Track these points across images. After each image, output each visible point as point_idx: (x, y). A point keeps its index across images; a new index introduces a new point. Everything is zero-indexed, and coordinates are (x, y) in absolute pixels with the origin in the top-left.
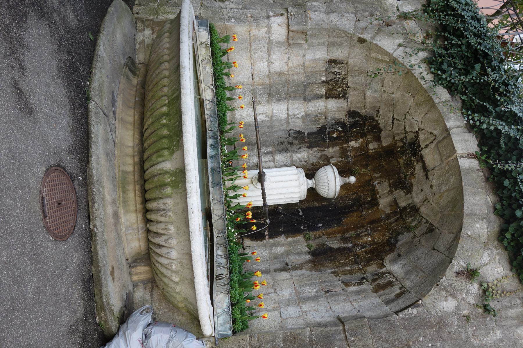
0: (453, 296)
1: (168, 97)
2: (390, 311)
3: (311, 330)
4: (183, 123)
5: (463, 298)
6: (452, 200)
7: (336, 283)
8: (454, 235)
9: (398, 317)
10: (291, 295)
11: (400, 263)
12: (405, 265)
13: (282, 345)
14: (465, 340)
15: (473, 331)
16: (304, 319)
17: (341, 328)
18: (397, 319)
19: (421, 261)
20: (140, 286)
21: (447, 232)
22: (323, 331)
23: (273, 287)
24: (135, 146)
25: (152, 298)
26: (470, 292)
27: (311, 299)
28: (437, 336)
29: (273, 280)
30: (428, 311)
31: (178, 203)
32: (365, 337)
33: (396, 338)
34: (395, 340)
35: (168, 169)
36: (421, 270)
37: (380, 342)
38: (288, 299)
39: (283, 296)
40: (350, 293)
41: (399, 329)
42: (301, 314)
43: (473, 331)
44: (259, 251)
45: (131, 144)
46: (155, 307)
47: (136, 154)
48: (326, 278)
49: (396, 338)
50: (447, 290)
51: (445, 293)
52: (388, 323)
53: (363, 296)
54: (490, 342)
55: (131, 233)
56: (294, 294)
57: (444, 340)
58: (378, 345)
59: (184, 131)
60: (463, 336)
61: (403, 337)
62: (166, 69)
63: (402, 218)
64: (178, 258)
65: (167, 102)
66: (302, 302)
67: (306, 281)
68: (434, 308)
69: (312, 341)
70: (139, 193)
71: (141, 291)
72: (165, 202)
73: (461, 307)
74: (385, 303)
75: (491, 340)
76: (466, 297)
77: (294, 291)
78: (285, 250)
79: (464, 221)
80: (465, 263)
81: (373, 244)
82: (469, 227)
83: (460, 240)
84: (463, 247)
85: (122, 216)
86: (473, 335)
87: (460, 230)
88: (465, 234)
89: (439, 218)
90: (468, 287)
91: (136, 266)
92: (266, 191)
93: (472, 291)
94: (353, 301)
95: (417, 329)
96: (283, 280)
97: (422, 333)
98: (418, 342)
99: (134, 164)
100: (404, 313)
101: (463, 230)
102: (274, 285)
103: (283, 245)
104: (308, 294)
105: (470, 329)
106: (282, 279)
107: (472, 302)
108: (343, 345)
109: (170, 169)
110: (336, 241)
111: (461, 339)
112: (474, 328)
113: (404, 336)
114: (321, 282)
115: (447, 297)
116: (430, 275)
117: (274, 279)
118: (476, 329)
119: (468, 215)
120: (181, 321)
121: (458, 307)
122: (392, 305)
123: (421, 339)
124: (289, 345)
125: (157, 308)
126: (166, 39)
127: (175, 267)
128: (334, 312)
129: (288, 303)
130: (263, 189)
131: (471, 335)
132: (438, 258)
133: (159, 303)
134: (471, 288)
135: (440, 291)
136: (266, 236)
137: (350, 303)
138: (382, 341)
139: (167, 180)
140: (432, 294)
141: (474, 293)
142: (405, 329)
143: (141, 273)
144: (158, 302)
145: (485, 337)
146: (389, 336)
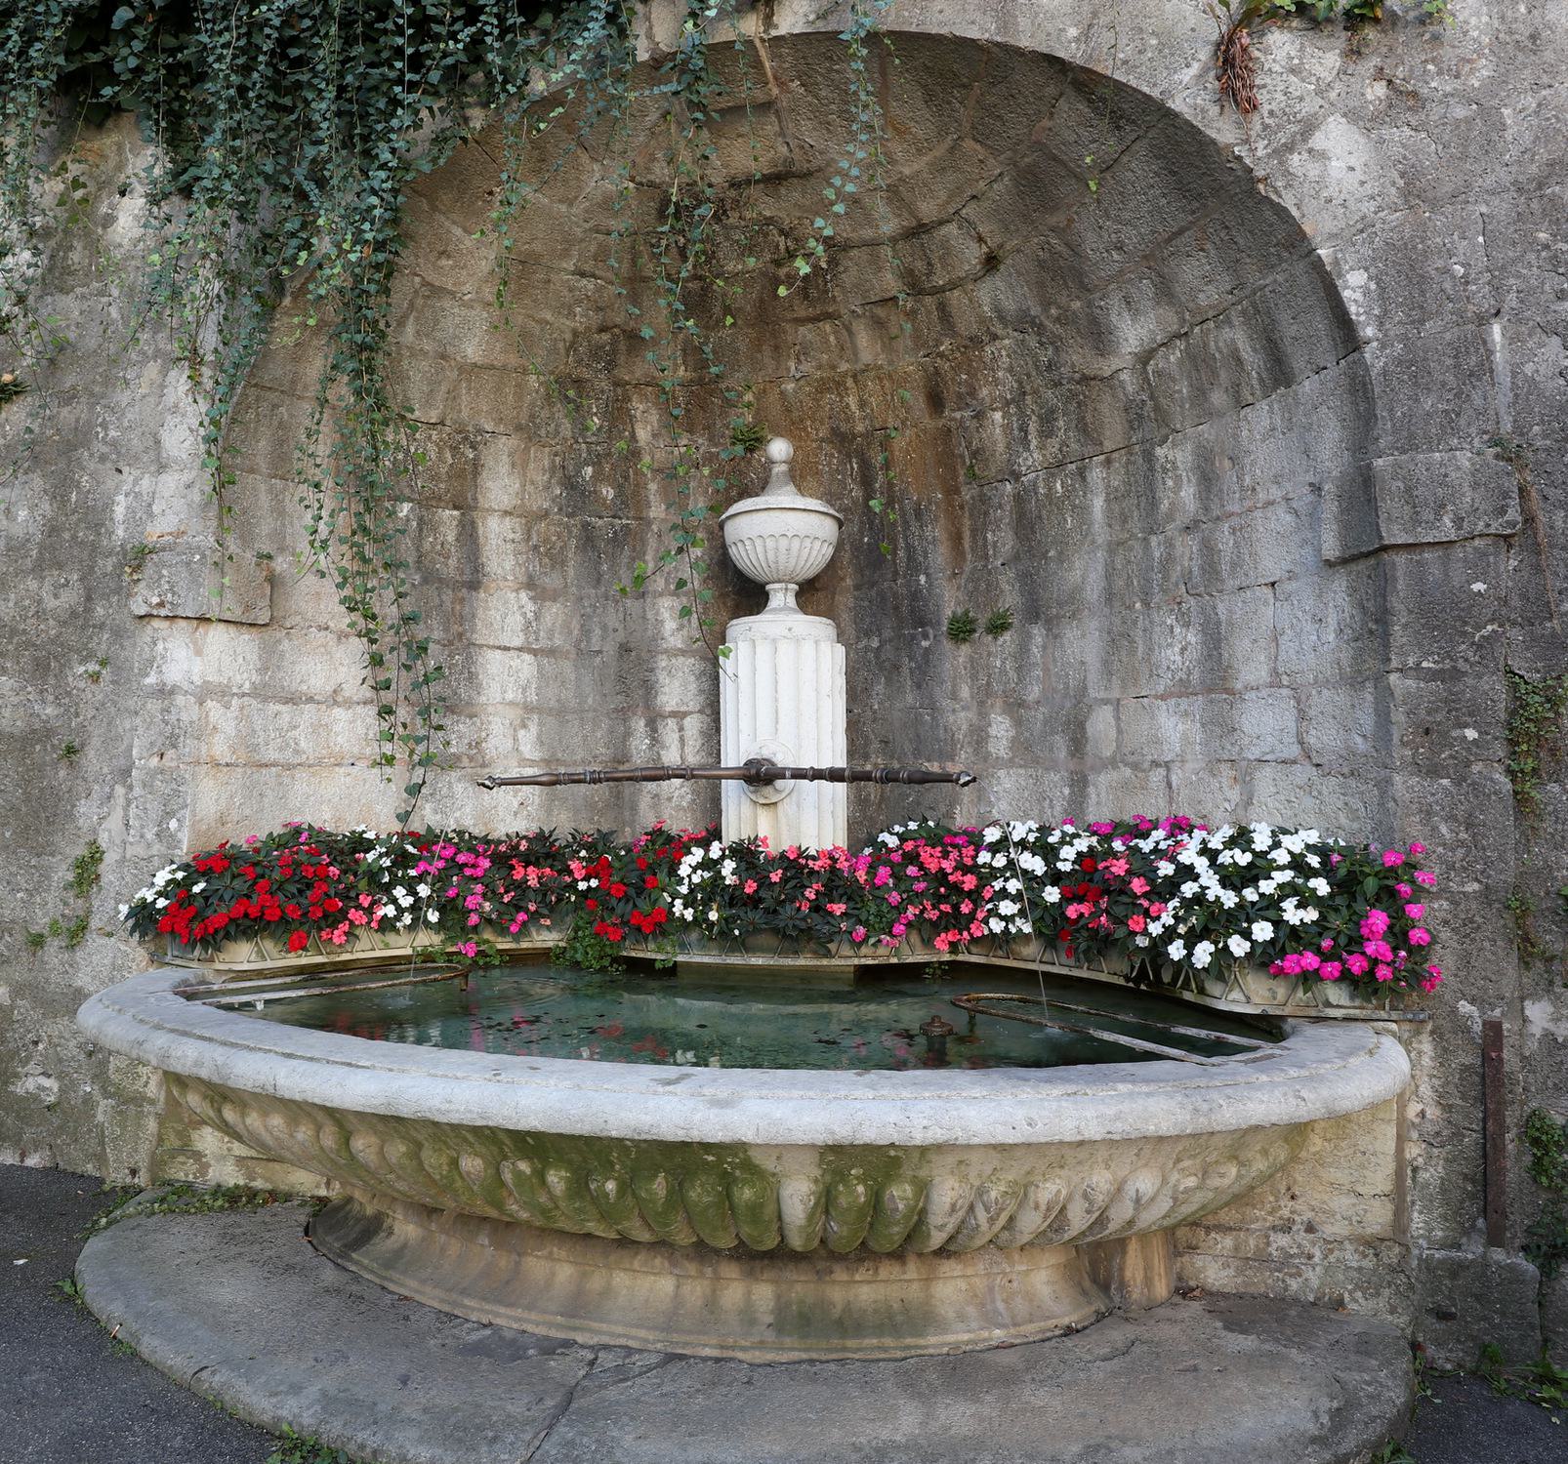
0: (1309, 127)
1: (505, 1158)
2: (1333, 372)
3: (1401, 671)
4: (644, 1137)
5: (1319, 92)
6: (924, 87)
7: (1157, 554)
8: (1070, 91)
9: (1375, 344)
10: (1186, 714)
11: (1114, 318)
12: (1128, 301)
13: (1445, 782)
14: (1475, 106)
15: (1440, 73)
16: (1320, 683)
17: (1400, 559)
18: (1383, 347)
19: (1131, 237)
20: (1182, 1269)
21: (1046, 123)
22: (1405, 626)
23: (1144, 771)
24: (676, 1271)
25: (1231, 1229)
26: (1296, 61)
27: (1217, 648)
28: (1450, 208)
29: (1115, 767)
30: (1360, 226)
31: (961, 1162)
32: (1446, 476)
33: (1449, 362)
34: (1457, 366)
35: (813, 1187)
36: (1169, 240)
37: (1462, 422)
38: (1203, 725)
39: (1185, 739)
40: (1207, 509)
41: (1419, 344)
42: (1285, 692)
43: (1440, 73)
44: (999, 799)
45: (666, 1285)
46: (1265, 1220)
47: (709, 1271)
48: (1129, 583)
49: (1449, 362)
50: (1284, 145)
51: (1296, 157)
52: (1395, 382)
53: (1227, 463)
54: (1485, 19)
55: (1005, 1301)
56: (1184, 703)
57: (1468, 185)
58: (1473, 430)
59: (681, 1136)
60: (1460, 112)
61: (1448, 336)
62: (382, 1148)
63: (942, 290)
64: (1162, 1168)
65: (524, 1166)
66: (1224, 679)
67: (1132, 652)
68: (1351, 203)
69: (1442, 670)
70: (862, 1270)
71: (1200, 1264)
72: (947, 1207)
73: (1351, 104)
74: (1275, 389)
75: (1478, 14)
76: (1313, 79)
77: (1173, 701)
78: (1004, 712)
79: (1025, 42)
80: (1188, 66)
81: (1018, 407)
82: (1050, 27)
83: (1099, 69)
84: (1125, 62)
85: (951, 1338)
86: (1456, 77)
87: (1058, 67)
88: (1078, 49)
89: (978, 147)
90: (1277, 68)
91: (1123, 1285)
92: (806, 764)
93: (1293, 54)
94: (1248, 504)
95: (1424, 278)
96: (1120, 731)
97: (1440, 264)
98: (1467, 283)
99: (750, 1275)
100: (1362, 318)
101: (1061, 54)
102: (1135, 767)
103: (983, 715)
104: (1193, 654)
105: (1433, 85)
106: (1113, 734)
107: (1332, 60)
108: (1465, 560)
109: (816, 1181)
110: (989, 536)
111: (1469, 121)
112: (1430, 67)
113: (1446, 329)
114: (1146, 604)
115: (1310, 151)
116: (1205, 206)
117: (1113, 763)
118: (1433, 60)
119: (1004, 27)
120: (1328, 1136)
121: (1353, 116)
122: (1298, 362)
123: (1459, 270)
124: (1451, 757)
125: (1270, 1213)
126: (248, 1121)
127: (1193, 1178)
128: (1292, 576)
129: (1221, 726)
130: (799, 774)
131: (1457, 84)
132: (1140, 170)
133: (1254, 1207)
134: (1280, 55)
135: (1287, 173)
136: (943, 768)
137: (1258, 514)
138: (1458, 415)
139: (858, 1196)
140: (1298, 207)
141: (1302, 49)
142: (1422, 322)
143: (1148, 1268)
144: (1248, 1210)
145: (1465, 33)
146: (1444, 384)
